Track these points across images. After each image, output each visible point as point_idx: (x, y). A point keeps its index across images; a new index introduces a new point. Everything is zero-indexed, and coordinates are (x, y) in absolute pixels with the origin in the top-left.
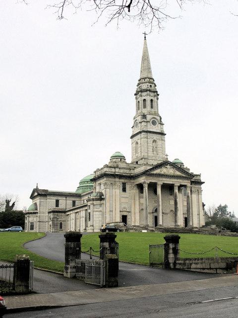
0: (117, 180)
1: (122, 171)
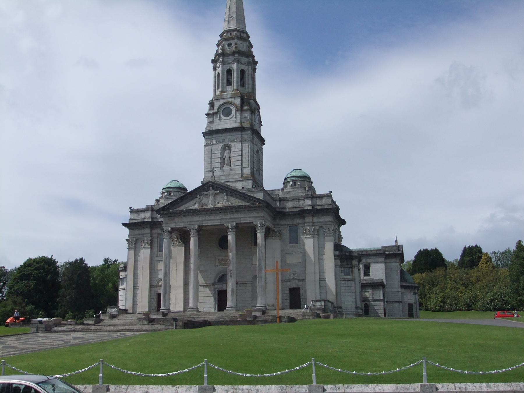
0: (147, 231)
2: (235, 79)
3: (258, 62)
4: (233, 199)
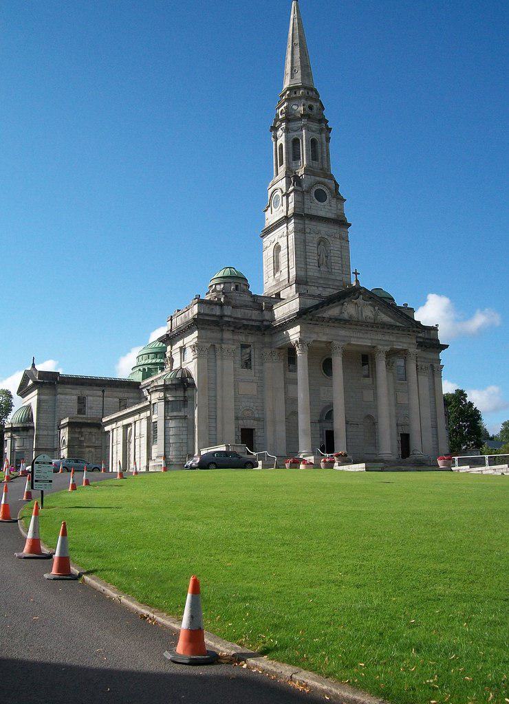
0: (227, 335)
1: (239, 313)
4: (383, 316)
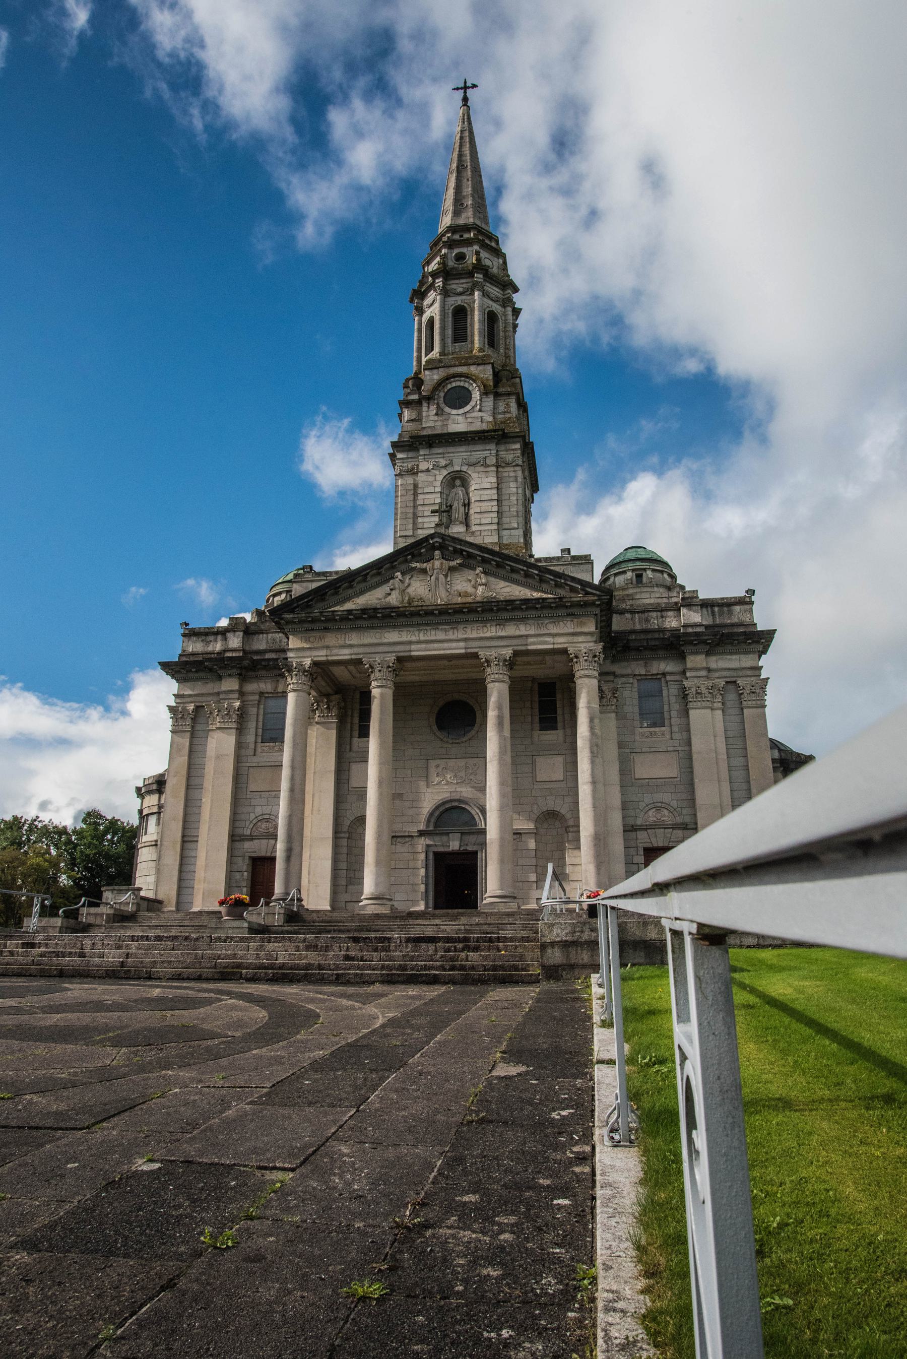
0: (230, 684)
2: (477, 326)
3: (521, 309)
4: (502, 584)
